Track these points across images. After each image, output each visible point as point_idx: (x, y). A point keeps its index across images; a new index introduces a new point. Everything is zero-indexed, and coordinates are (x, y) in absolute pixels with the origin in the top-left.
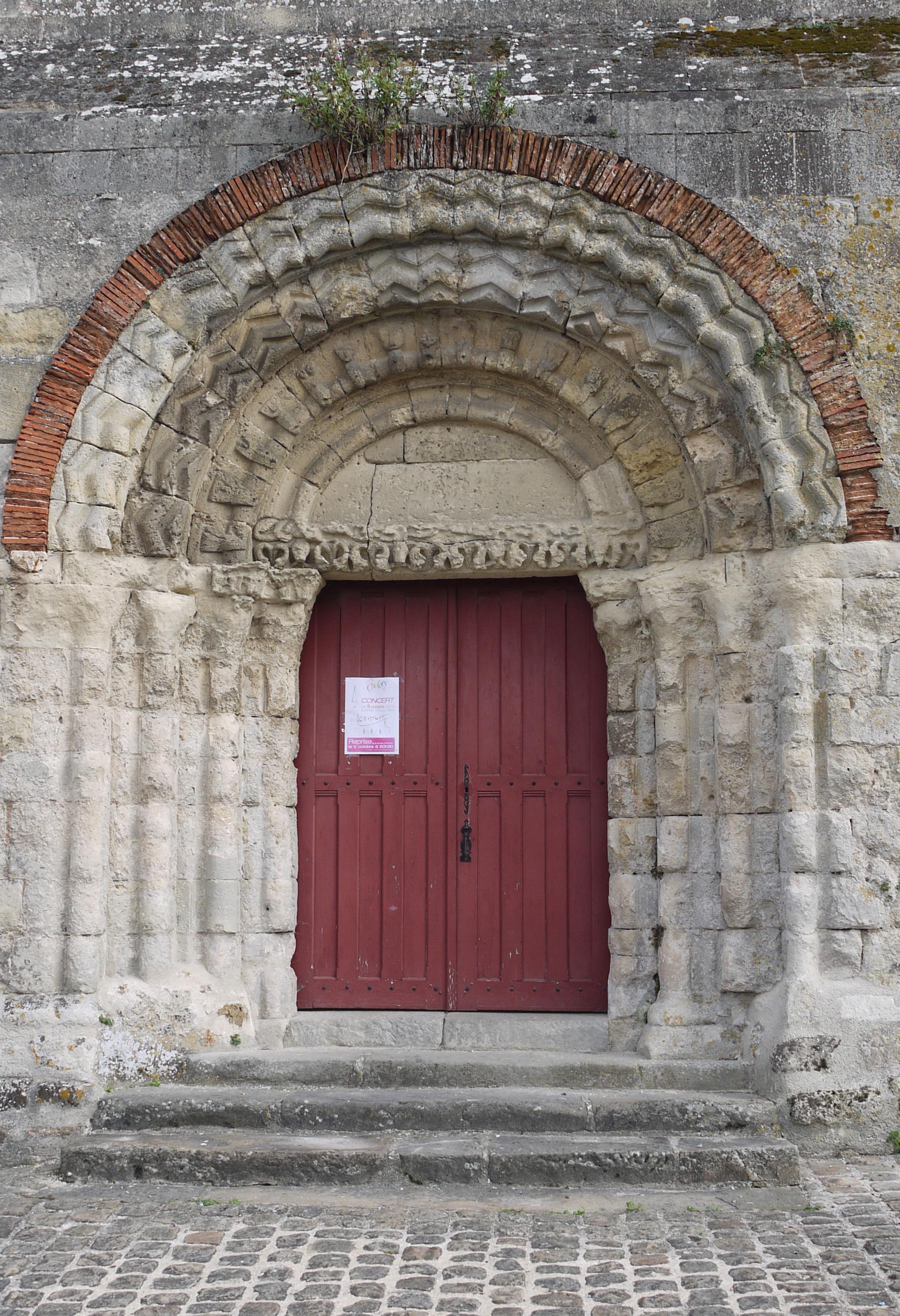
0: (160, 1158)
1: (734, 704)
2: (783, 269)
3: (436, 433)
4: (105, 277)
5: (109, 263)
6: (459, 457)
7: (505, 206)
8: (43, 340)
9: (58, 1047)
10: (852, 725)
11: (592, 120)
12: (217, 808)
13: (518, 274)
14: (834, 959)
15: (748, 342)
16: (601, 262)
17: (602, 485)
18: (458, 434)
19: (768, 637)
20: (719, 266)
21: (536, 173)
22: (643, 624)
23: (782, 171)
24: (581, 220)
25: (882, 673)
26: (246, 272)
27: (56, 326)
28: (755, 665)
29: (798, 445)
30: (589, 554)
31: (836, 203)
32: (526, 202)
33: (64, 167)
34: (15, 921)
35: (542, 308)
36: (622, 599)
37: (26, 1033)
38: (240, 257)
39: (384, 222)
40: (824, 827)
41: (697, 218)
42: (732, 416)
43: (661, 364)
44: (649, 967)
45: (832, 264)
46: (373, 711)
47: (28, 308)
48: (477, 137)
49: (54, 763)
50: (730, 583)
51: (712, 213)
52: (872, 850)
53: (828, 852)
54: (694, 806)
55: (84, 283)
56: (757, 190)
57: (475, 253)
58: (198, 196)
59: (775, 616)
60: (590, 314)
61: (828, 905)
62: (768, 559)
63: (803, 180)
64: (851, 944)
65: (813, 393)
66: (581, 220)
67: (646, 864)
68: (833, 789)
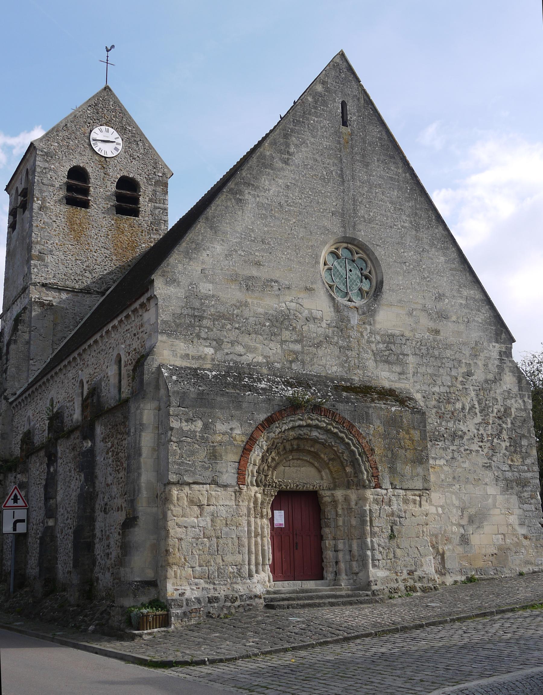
0: (291, 605)
1: (353, 518)
2: (364, 438)
3: (295, 461)
4: (253, 429)
5: (254, 426)
6: (299, 466)
7: (320, 422)
8: (243, 441)
9: (253, 588)
10: (376, 523)
11: (334, 406)
12: (264, 539)
13: (319, 434)
14: (374, 566)
15: (358, 451)
16: (336, 434)
17: (325, 473)
18: (299, 462)
19: (359, 505)
20: (354, 436)
21: (326, 416)
22: (335, 502)
23: (363, 419)
24: (332, 425)
25: (380, 513)
26: (278, 430)
27: (245, 439)
28: (356, 511)
29: (366, 470)
30: (323, 487)
31: (371, 426)
32: (324, 421)
33: (245, 405)
34: (241, 562)
35: (323, 441)
36: (329, 496)
37: (246, 585)
38: (277, 427)
39: (301, 423)
40: (372, 541)
41: (351, 426)
42: (354, 463)
43: (343, 453)
44: (335, 570)
45: (371, 437)
46: (280, 517)
47: (239, 434)
48: (317, 408)
49: (246, 529)
50: (353, 495)
51: (353, 426)
52: (379, 546)
53: (373, 546)
54: (343, 538)
55: (250, 430)
56: (360, 422)
57: (313, 429)
58: (269, 414)
59: (360, 502)
60: (331, 442)
61: (373, 556)
62: (359, 491)
63: (366, 421)
64: (377, 563)
65: (368, 461)
66: (332, 425)
67: (333, 549)
68: (373, 534)
